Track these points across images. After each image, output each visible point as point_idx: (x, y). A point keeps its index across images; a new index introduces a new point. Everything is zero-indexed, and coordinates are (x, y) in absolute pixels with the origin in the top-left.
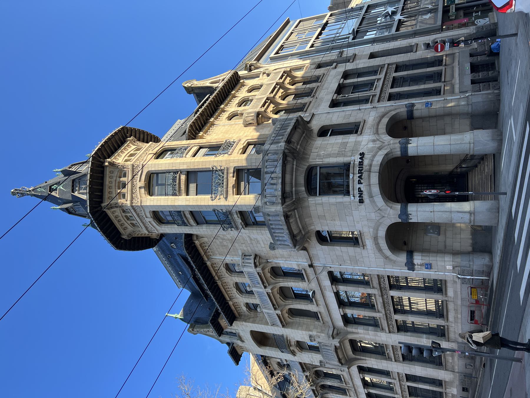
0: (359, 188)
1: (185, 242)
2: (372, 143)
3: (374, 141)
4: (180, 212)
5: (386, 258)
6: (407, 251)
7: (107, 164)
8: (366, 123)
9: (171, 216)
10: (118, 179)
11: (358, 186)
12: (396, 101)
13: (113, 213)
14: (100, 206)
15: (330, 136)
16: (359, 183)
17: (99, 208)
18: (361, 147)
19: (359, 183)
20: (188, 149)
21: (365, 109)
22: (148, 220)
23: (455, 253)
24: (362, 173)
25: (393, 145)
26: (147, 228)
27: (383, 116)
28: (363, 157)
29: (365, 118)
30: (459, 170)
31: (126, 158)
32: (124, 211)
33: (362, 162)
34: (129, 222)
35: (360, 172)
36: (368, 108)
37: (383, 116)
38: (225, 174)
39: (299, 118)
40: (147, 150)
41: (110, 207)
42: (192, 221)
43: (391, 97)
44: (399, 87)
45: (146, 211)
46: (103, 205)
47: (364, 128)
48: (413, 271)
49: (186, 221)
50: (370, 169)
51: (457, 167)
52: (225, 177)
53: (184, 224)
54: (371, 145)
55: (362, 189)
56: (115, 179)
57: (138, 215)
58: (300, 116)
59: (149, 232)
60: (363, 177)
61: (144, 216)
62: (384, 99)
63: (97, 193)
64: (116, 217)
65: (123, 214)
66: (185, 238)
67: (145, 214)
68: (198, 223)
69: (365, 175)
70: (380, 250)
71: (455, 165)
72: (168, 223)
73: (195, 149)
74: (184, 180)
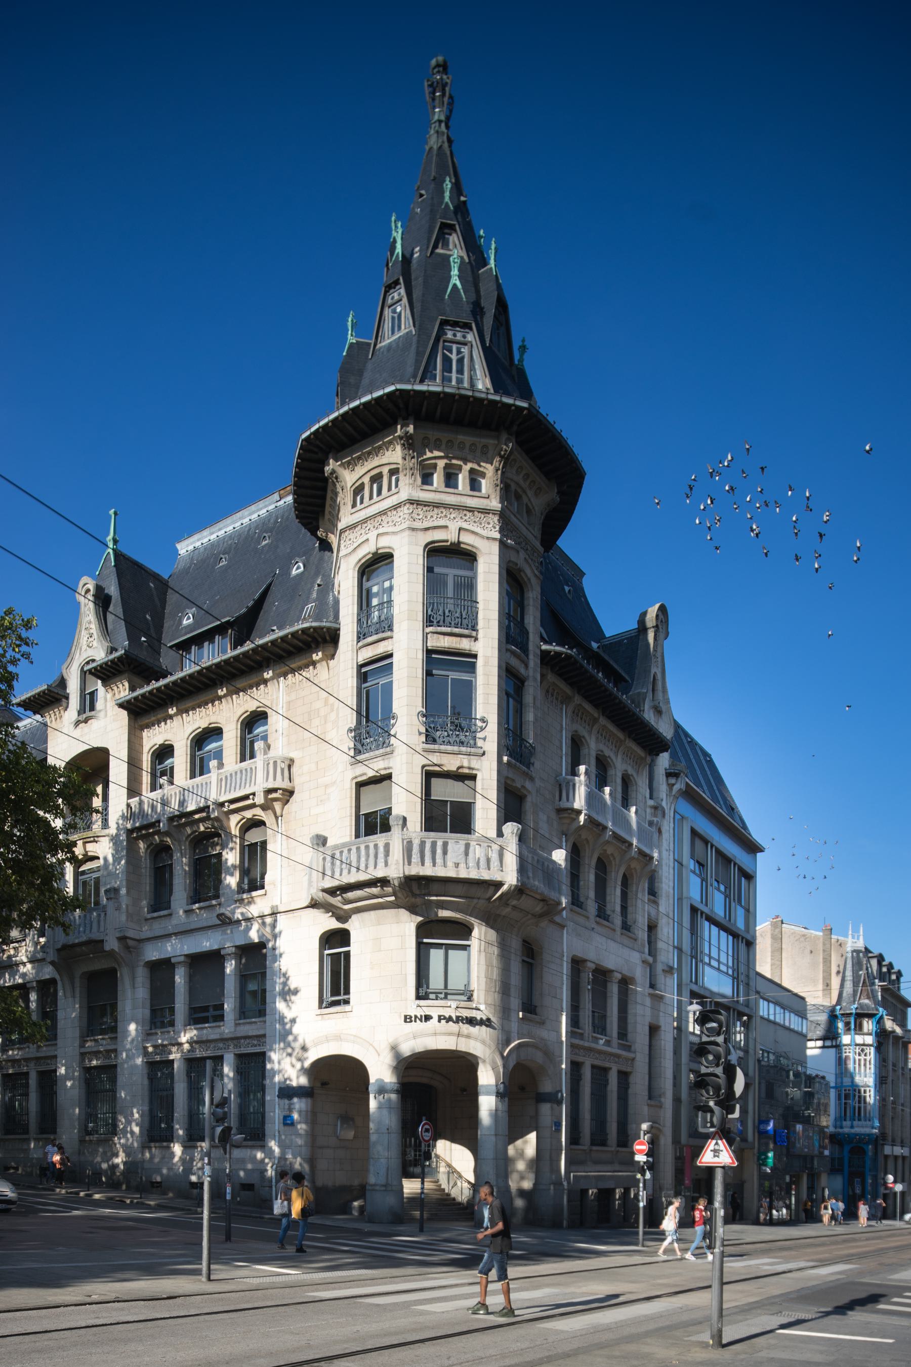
4: (390, 628)
42: (367, 654)
43: (575, 1066)
44: (592, 1078)
45: (394, 537)
48: (278, 1096)
49: (370, 639)
57: (383, 513)
61: (381, 530)
62: (576, 1054)
65: (385, 470)
66: (329, 629)
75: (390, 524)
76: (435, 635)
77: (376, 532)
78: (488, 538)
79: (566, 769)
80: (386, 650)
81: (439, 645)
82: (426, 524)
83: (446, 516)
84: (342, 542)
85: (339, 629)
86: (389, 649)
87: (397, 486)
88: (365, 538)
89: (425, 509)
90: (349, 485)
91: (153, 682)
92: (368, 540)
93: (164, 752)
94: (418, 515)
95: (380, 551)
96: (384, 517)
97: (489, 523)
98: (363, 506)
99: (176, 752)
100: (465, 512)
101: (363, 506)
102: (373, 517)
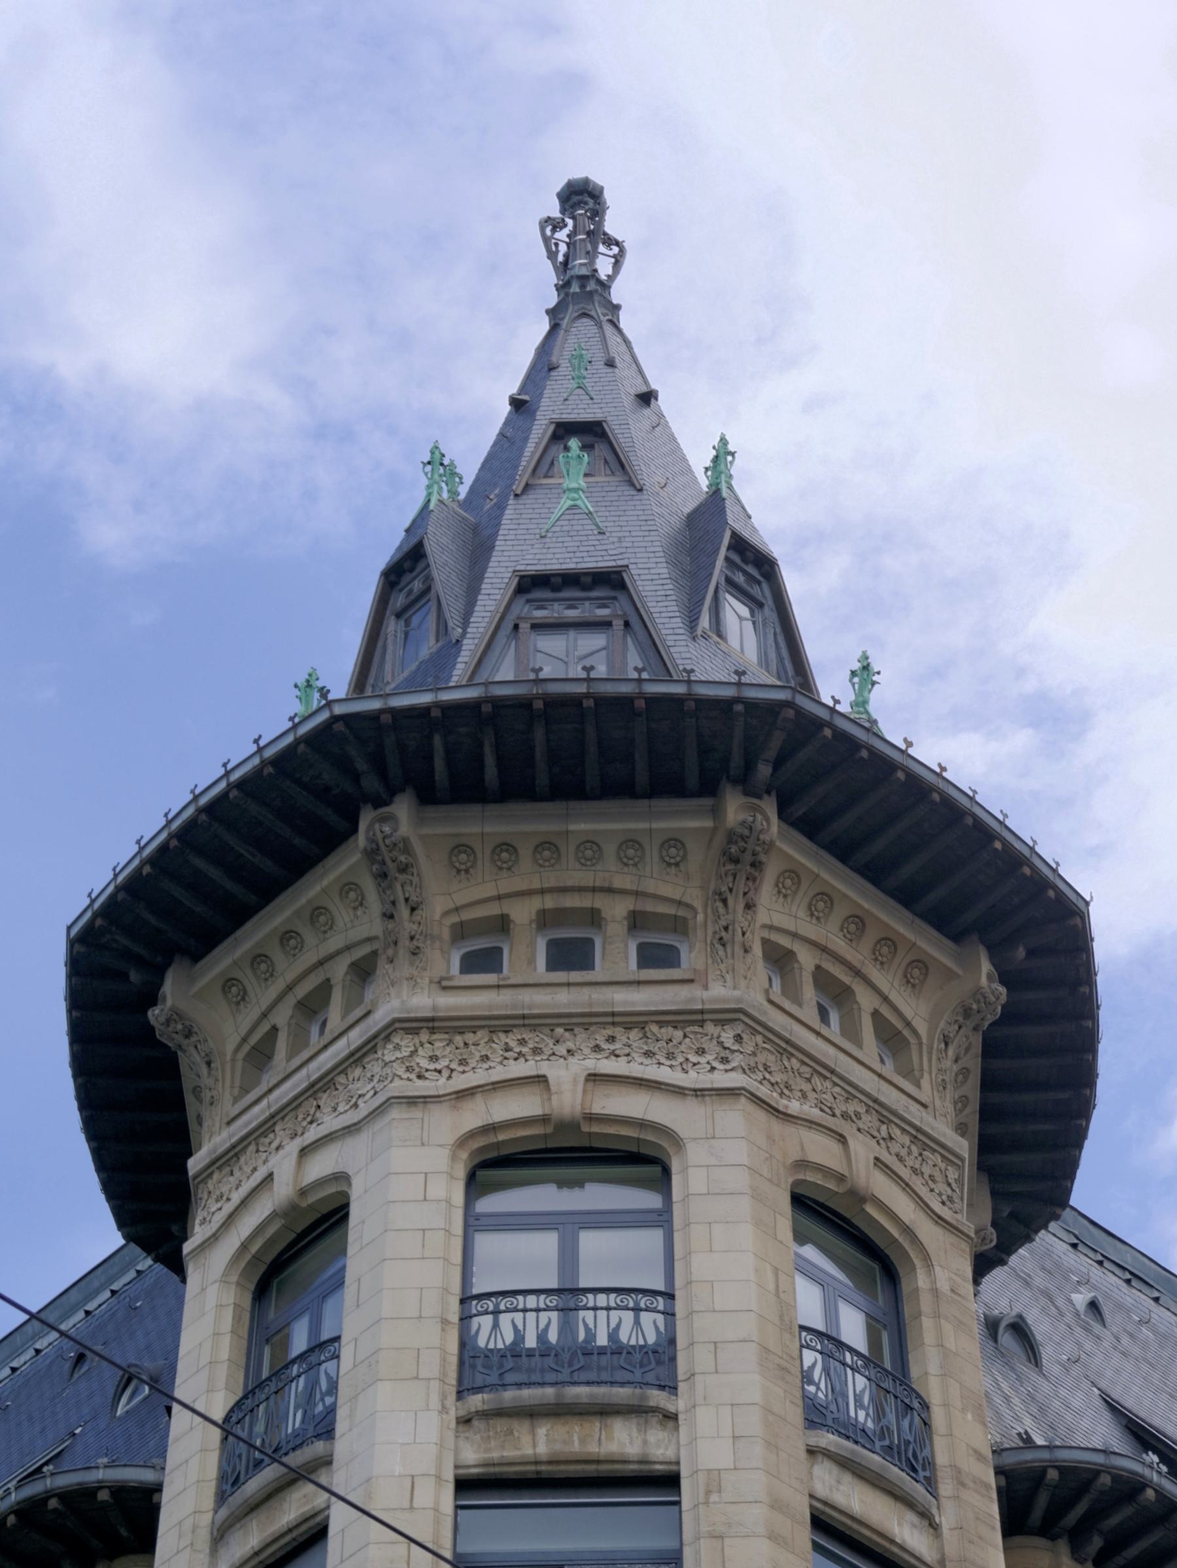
1: (87, 1493)
10: (616, 910)
13: (348, 887)
17: (370, 783)
26: (228, 1158)
34: (282, 1016)
41: (389, 867)
46: (403, 809)
56: (622, 881)
63: (490, 761)
64: (317, 914)
65: (339, 970)
67: (329, 1138)
74: (593, 1449)
75: (341, 1109)
76: (501, 1424)
77: (298, 1143)
78: (699, 1093)
80: (306, 1509)
81: (510, 1453)
82: (461, 1081)
83: (536, 1051)
89: (458, 1039)
92: (270, 1177)
94: (433, 1058)
95: (312, 1199)
97: (701, 1052)
100: (609, 1032)
102: (294, 1105)
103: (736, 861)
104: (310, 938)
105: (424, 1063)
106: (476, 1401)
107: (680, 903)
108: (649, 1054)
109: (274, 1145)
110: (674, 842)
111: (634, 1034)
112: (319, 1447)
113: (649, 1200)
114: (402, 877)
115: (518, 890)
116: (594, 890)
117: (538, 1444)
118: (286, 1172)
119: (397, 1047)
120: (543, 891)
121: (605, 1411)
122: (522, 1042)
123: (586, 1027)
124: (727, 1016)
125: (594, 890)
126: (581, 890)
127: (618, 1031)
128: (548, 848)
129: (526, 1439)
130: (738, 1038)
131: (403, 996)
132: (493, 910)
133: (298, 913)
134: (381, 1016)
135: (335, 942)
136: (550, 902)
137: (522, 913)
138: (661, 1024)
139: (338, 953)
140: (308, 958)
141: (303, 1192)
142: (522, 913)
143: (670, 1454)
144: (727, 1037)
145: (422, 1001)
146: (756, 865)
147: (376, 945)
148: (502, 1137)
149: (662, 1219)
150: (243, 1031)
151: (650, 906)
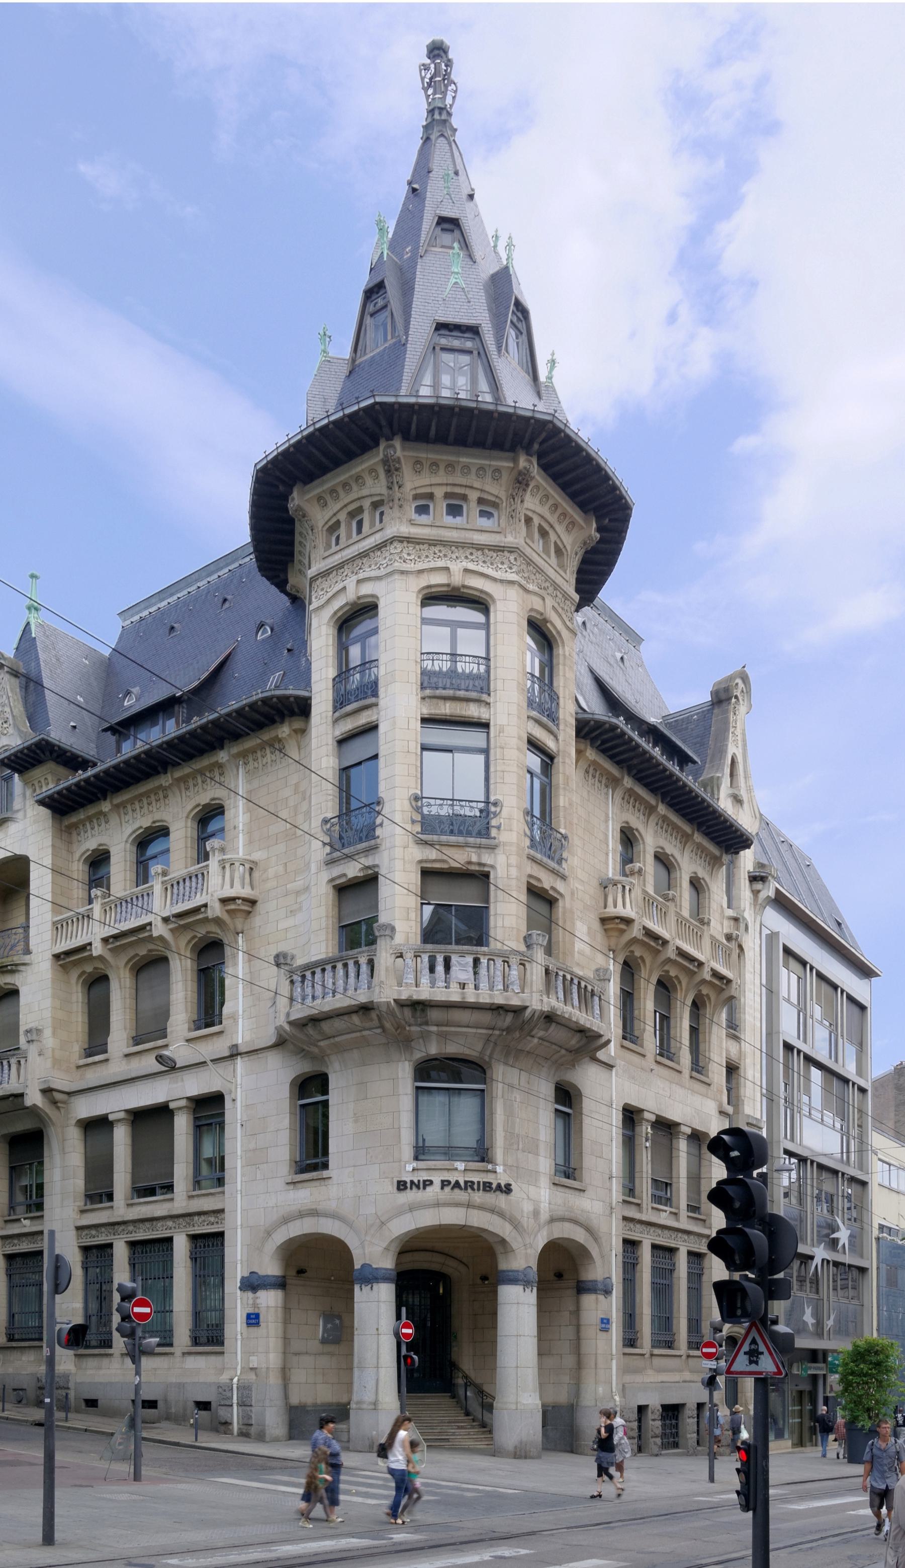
0: (431, 1182)
2: (531, 1208)
3: (536, 1213)
4: (375, 694)
5: (269, 1233)
6: (284, 1277)
7: (523, 462)
8: (577, 1193)
9: (363, 664)
10: (473, 496)
11: (437, 1179)
12: (620, 1258)
13: (372, 470)
14: (394, 434)
15: (556, 1110)
16: (443, 1181)
18: (524, 1186)
19: (443, 1181)
20: (550, 724)
21: (610, 1190)
22: (350, 583)
23: (285, 1372)
24: (466, 1189)
25: (524, 1255)
26: (325, 574)
27: (588, 1229)
28: (501, 1191)
29: (590, 1192)
30: (460, 1381)
31: (536, 521)
32: (376, 505)
33: (490, 1187)
35: (469, 1185)
36: (611, 1197)
37: (588, 1229)
38: (478, 840)
39: (603, 1040)
40: (556, 586)
41: (391, 468)
42: (348, 725)
47: (567, 1190)
48: (241, 1289)
49: (349, 708)
50: (474, 1207)
51: (466, 1377)
52: (471, 840)
53: (340, 702)
54: (527, 1207)
55: (429, 1189)
58: (609, 1041)
59: (313, 580)
60: (457, 1191)
61: (361, 575)
64: (358, 478)
65: (367, 504)
66: (297, 698)
67: (369, 579)
68: (342, 742)
69: (460, 1196)
70: (286, 1220)
71: (472, 1374)
72: (342, 649)
73: (550, 743)
74: (464, 713)
75: (373, 567)
76: (435, 701)
77: (355, 578)
78: (502, 581)
79: (614, 869)
81: (438, 712)
82: (420, 566)
83: (445, 556)
84: (313, 593)
85: (310, 698)
86: (374, 718)
87: (381, 521)
88: (340, 586)
89: (417, 547)
90: (321, 524)
91: (80, 772)
92: (345, 588)
93: (98, 861)
94: (409, 554)
95: (362, 601)
96: (365, 560)
97: (502, 563)
98: (338, 548)
99: (113, 860)
100: (470, 550)
101: (338, 548)
102: (352, 560)
103: (520, 483)
104: (355, 488)
105: (406, 556)
106: (428, 692)
107: (497, 497)
108: (484, 562)
109: (345, 574)
110: (498, 470)
111: (480, 553)
112: (373, 700)
113: (479, 617)
114: (396, 473)
115: (437, 482)
116: (466, 486)
117: (447, 709)
118: (351, 589)
119: (395, 548)
120: (447, 485)
121: (468, 700)
122: (440, 551)
123: (463, 547)
124: (512, 550)
125: (466, 486)
126: (461, 486)
127: (474, 551)
128: (450, 467)
129: (443, 707)
130: (515, 559)
131: (396, 527)
132: (428, 490)
133: (351, 477)
134: (389, 532)
135: (365, 492)
136: (449, 489)
137: (439, 492)
138: (489, 550)
139: (367, 496)
140: (353, 496)
141: (359, 598)
142: (439, 492)
143: (487, 717)
144: (512, 558)
145: (405, 529)
146: (527, 485)
147: (383, 498)
148: (433, 590)
149: (487, 626)
150: (327, 518)
151: (485, 496)
